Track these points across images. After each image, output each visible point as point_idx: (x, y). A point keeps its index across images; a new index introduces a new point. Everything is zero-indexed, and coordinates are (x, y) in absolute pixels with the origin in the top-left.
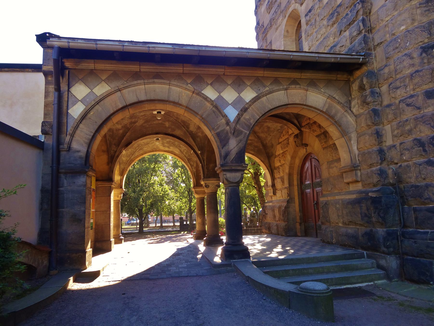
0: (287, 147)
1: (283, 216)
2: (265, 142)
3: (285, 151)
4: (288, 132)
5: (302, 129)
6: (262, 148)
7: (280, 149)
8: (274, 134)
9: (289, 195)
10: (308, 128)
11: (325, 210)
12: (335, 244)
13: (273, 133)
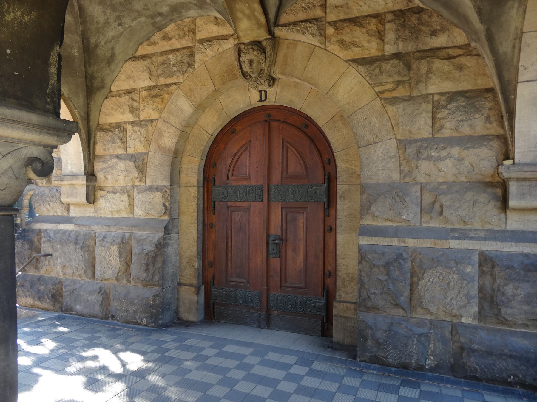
0: (183, 74)
1: (147, 270)
2: (93, 40)
3: (169, 85)
4: (194, 32)
5: (278, 32)
6: (76, 54)
7: (146, 75)
8: (135, 22)
9: (168, 210)
10: (317, 33)
11: (397, 273)
12: (431, 370)
13: (135, 19)
